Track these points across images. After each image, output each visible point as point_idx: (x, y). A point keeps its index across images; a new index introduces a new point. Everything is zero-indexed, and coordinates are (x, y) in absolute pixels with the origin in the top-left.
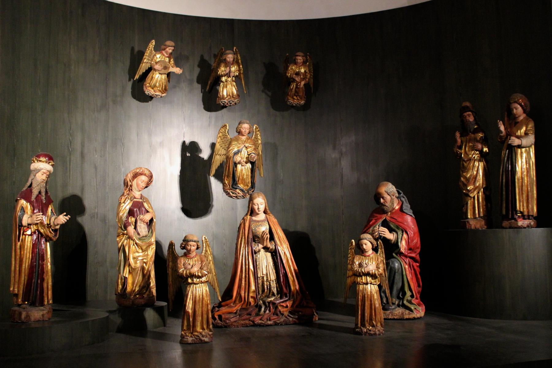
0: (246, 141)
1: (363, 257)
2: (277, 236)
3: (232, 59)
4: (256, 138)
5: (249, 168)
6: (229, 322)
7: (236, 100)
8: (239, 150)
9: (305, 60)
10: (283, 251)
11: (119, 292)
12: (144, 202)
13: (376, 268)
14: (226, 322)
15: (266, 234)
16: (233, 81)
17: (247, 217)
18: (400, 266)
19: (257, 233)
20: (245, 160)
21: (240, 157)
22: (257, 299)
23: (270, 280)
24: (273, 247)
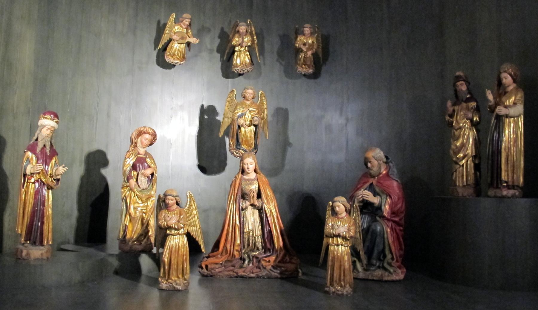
0: (250, 106)
1: (336, 219)
3: (245, 31)
4: (262, 102)
5: (252, 131)
6: (214, 272)
7: (248, 68)
8: (243, 113)
9: (312, 31)
10: (269, 209)
11: (121, 237)
12: (147, 158)
13: (347, 230)
14: (211, 272)
15: (252, 192)
16: (246, 51)
17: (239, 176)
18: (382, 229)
20: (248, 123)
21: (244, 120)
23: (256, 236)
24: (260, 205)
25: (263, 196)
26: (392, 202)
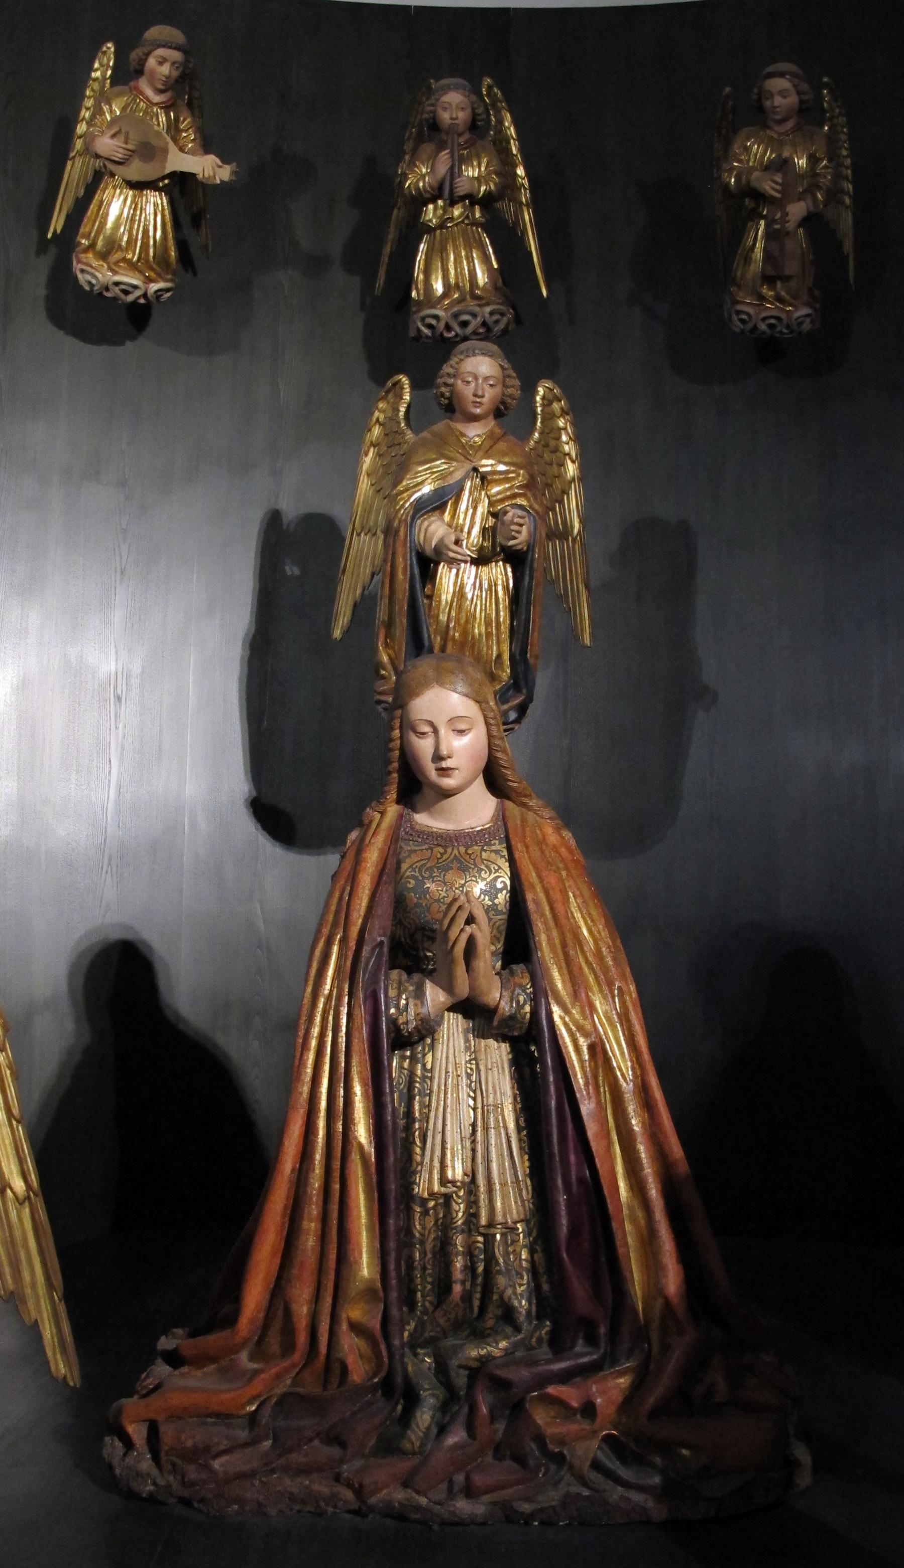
2: (555, 934)
3: (463, 116)
5: (500, 588)
6: (204, 1475)
7: (488, 309)
9: (806, 97)
10: (586, 1035)
15: (463, 916)
16: (475, 223)
17: (382, 814)
19: (428, 911)
22: (389, 1346)
23: (491, 1224)
24: (520, 1007)
25: (544, 944)
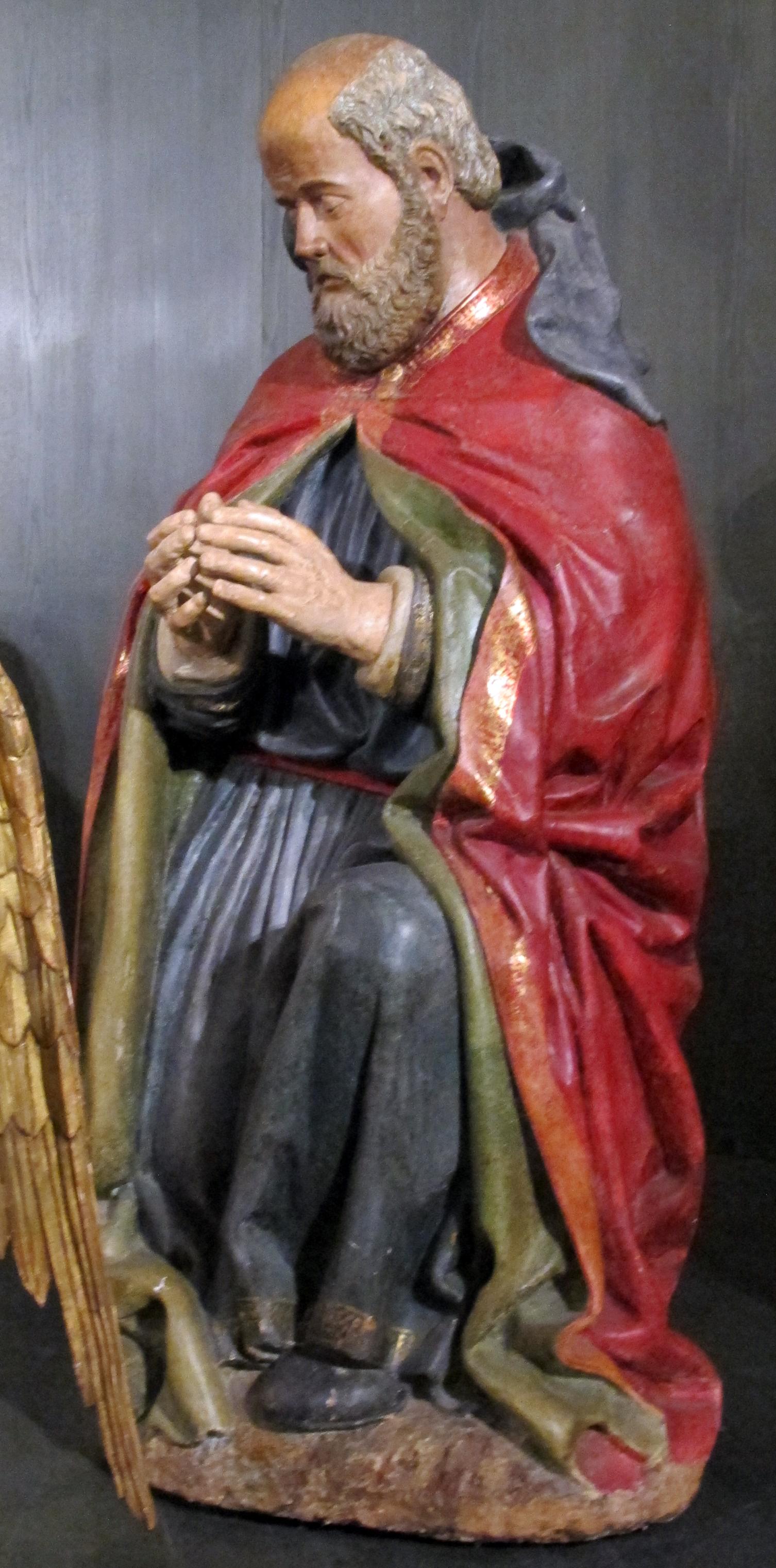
18: (443, 949)
26: (558, 628)
